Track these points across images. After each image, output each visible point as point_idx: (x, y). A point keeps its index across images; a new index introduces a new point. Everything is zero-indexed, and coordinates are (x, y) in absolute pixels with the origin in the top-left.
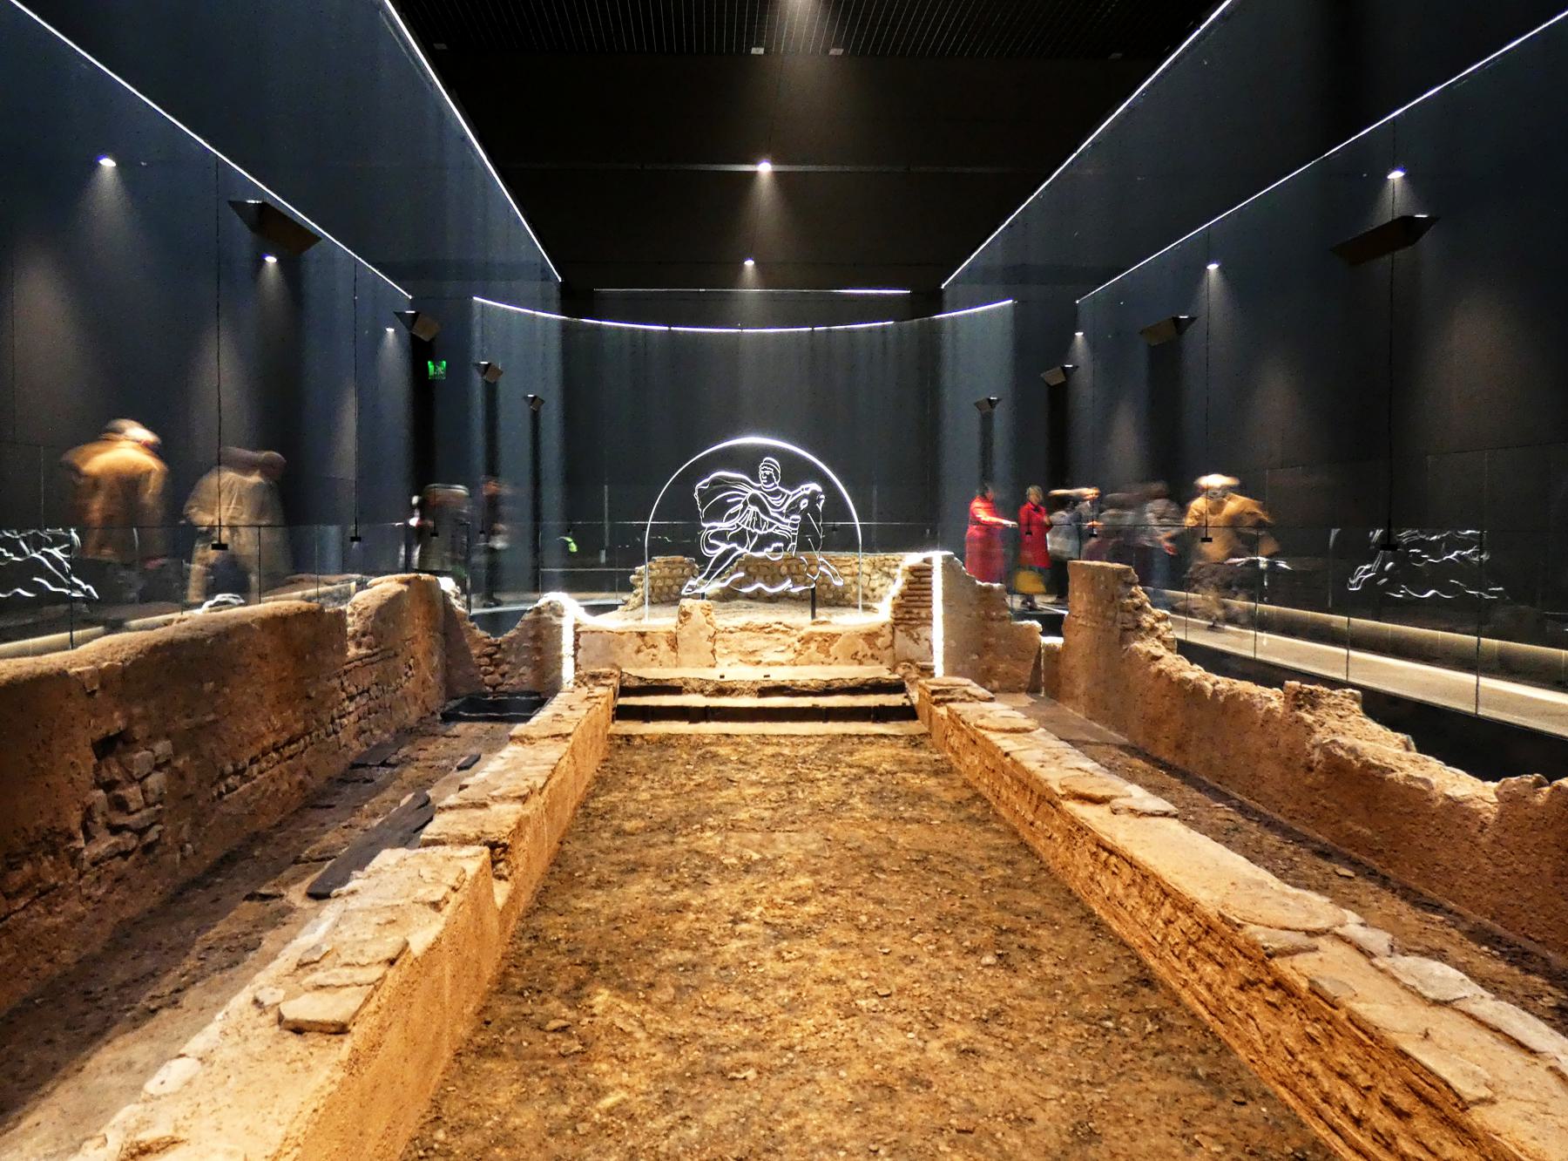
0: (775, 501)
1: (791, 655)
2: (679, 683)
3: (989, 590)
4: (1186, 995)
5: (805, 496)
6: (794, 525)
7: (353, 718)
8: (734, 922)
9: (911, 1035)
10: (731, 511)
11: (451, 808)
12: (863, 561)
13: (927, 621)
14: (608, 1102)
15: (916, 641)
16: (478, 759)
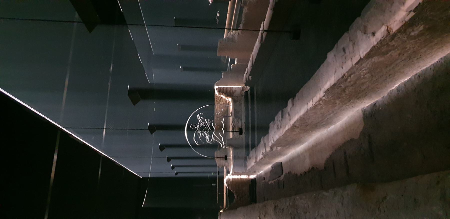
0: (201, 125)
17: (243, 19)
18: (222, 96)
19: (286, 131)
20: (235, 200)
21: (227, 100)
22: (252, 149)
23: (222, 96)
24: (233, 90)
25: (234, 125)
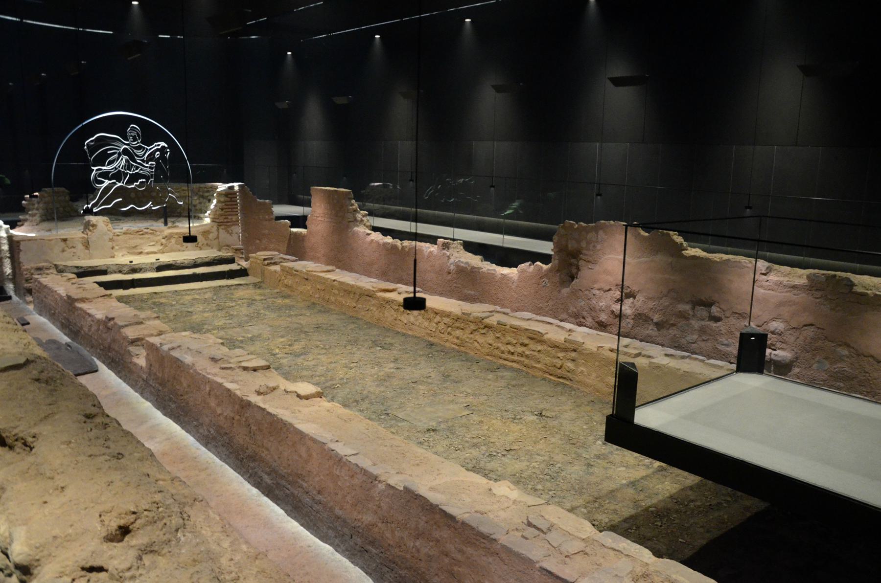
0: (139, 153)
2: (104, 268)
3: (265, 203)
4: (447, 345)
5: (157, 150)
6: (150, 168)
15: (231, 234)
17: (406, 243)
18: (215, 201)
19: (221, 385)
21: (207, 214)
22: (101, 284)
23: (215, 201)
25: (147, 233)
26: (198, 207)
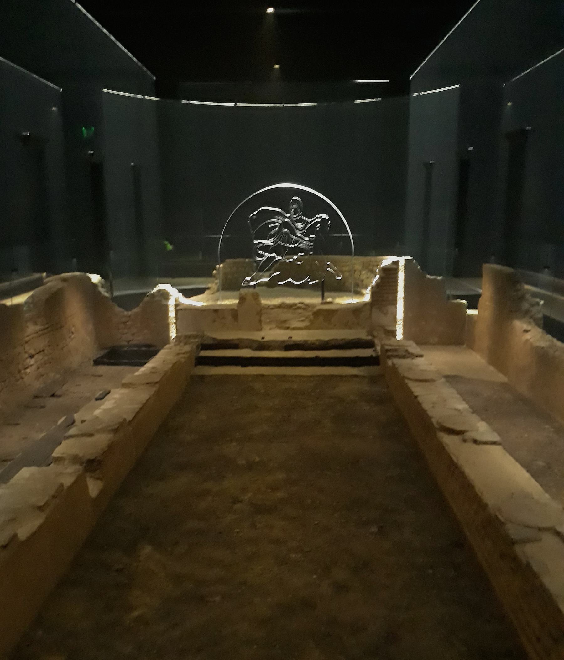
0: (300, 225)
1: (307, 323)
7: (34, 368)
8: (234, 503)
9: (315, 576)
10: (273, 232)
11: (71, 436)
12: (357, 262)
13: (394, 302)
14: (136, 614)
16: (109, 393)
18: (377, 277)
20: (120, 309)
24: (390, 308)
25: (299, 308)
26: (365, 282)
